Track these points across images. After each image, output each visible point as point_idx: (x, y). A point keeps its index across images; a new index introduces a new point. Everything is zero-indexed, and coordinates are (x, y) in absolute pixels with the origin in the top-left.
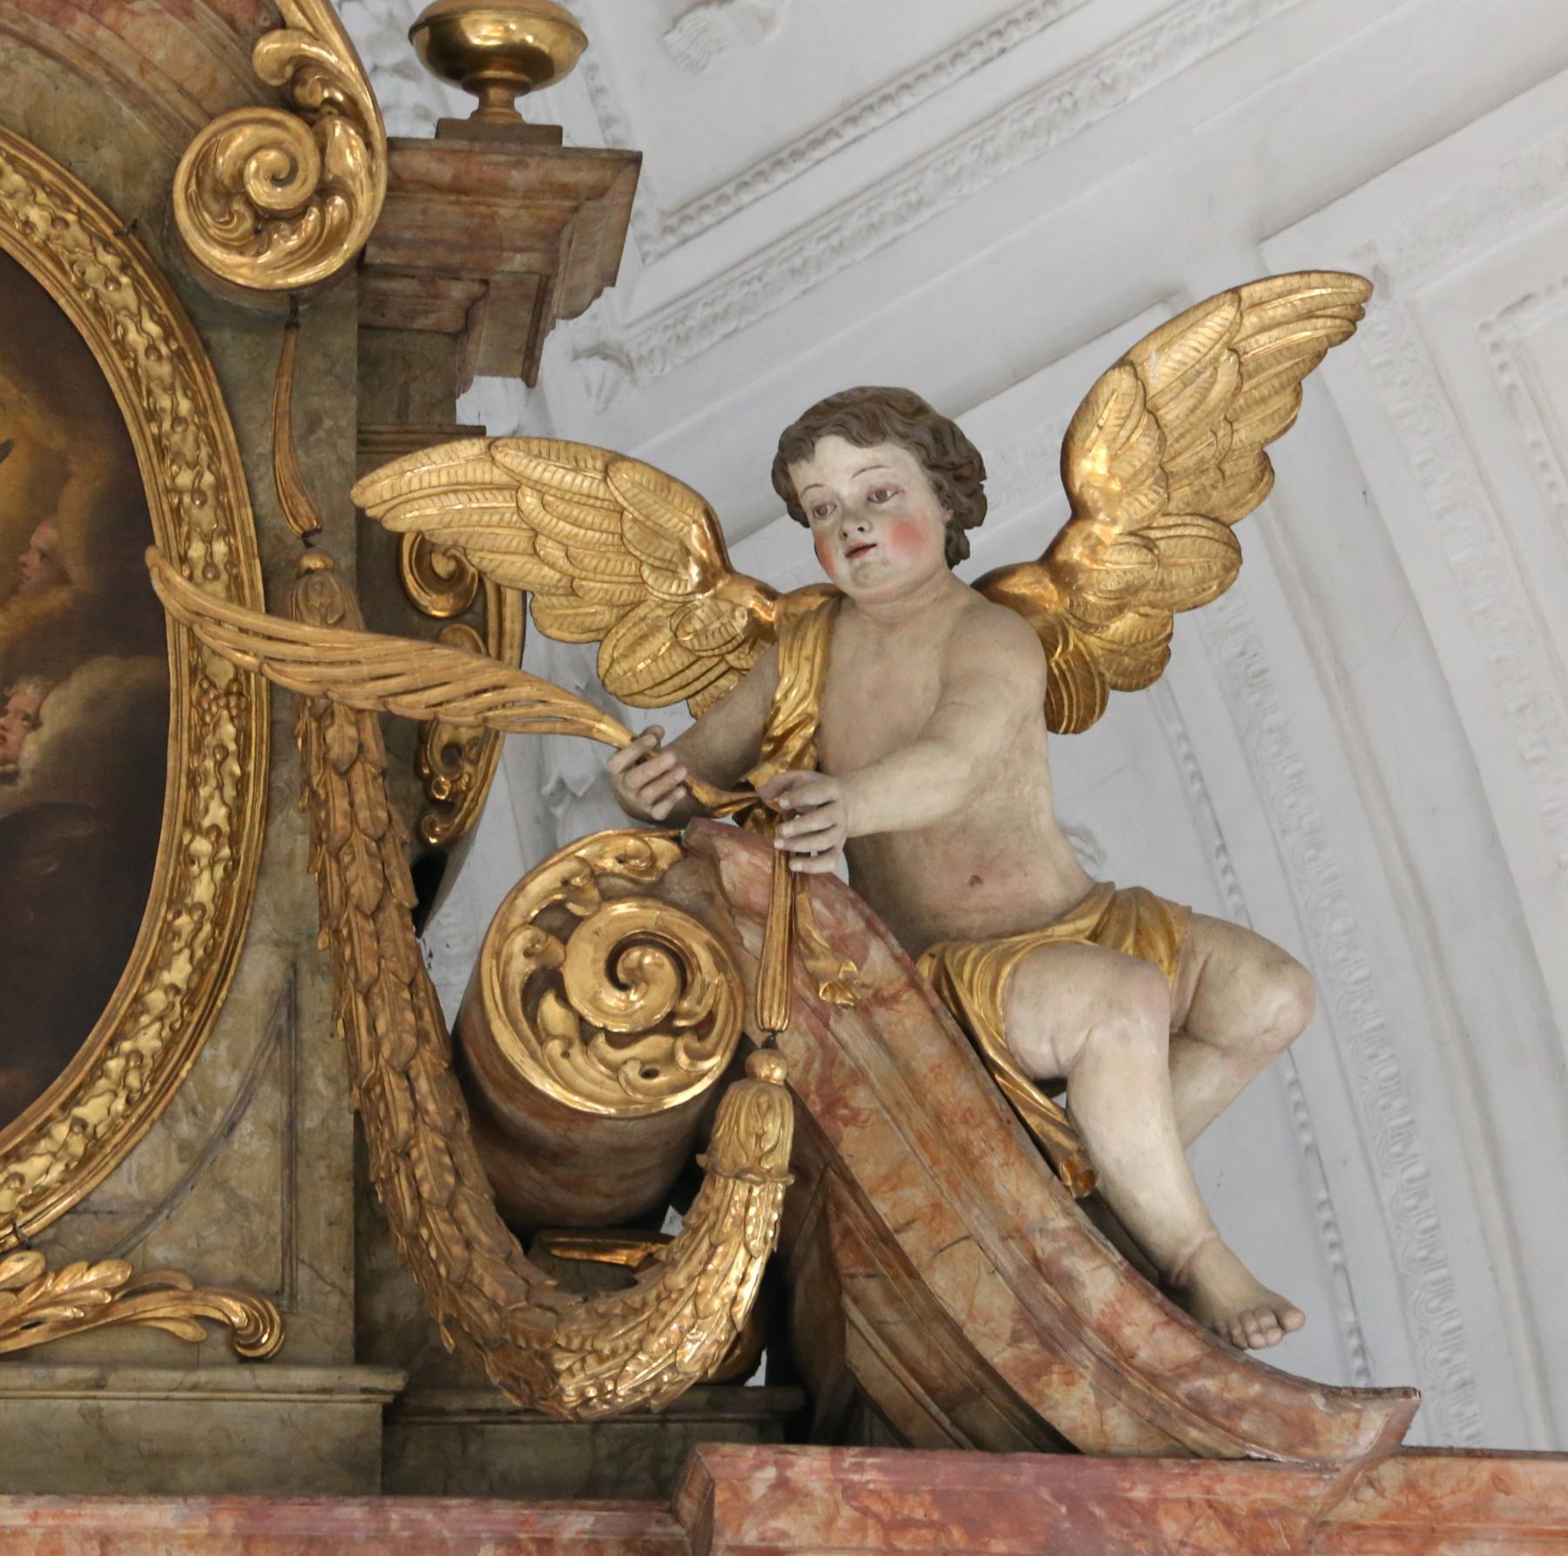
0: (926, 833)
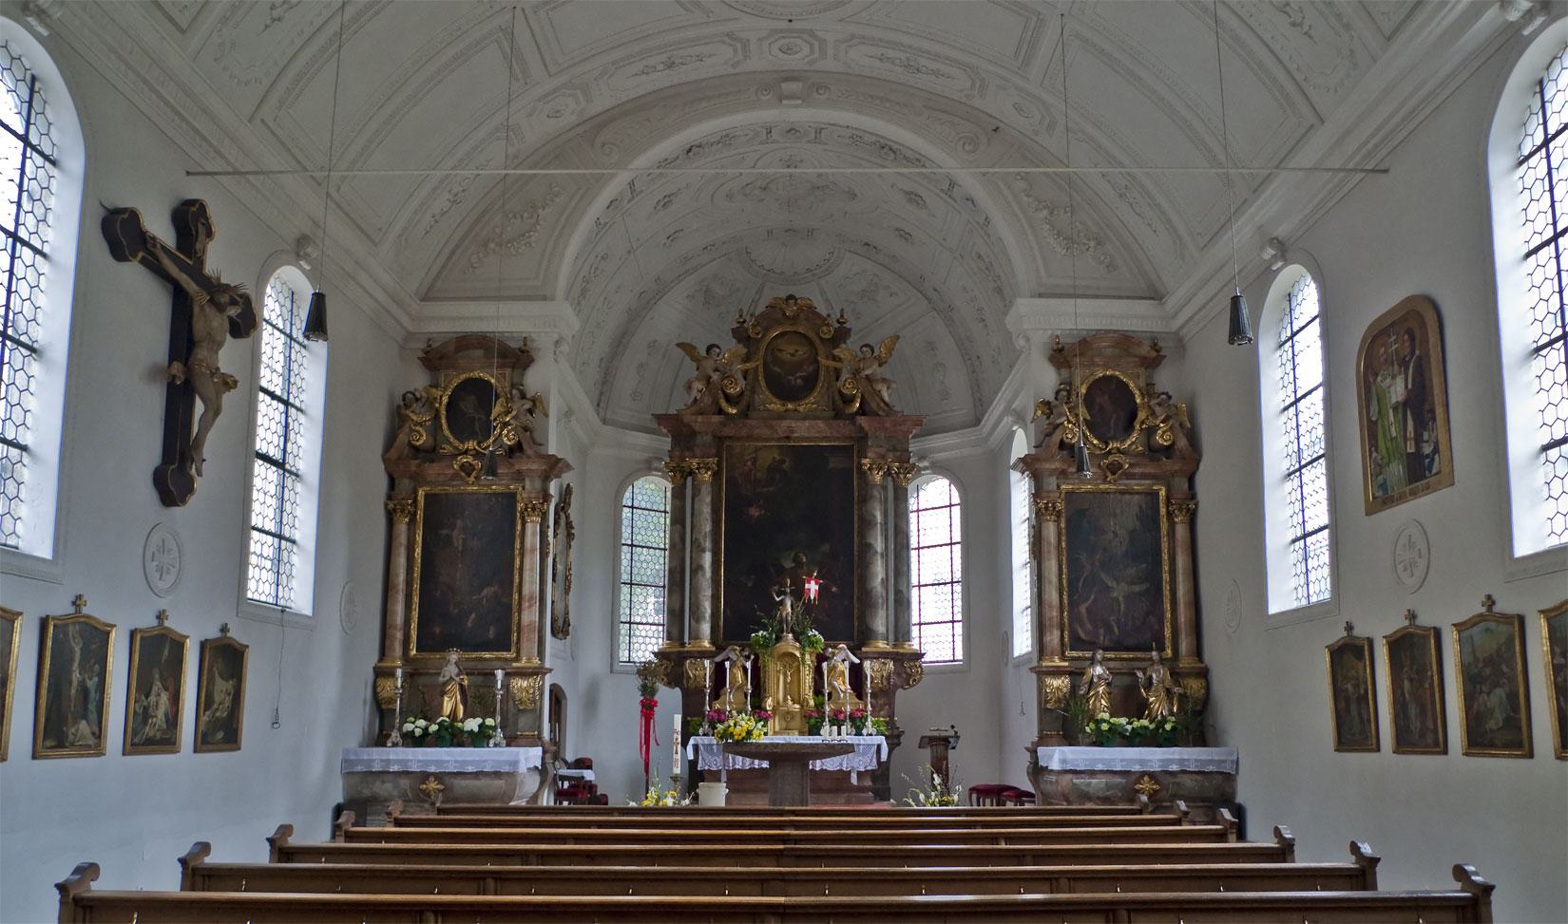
0: (872, 374)
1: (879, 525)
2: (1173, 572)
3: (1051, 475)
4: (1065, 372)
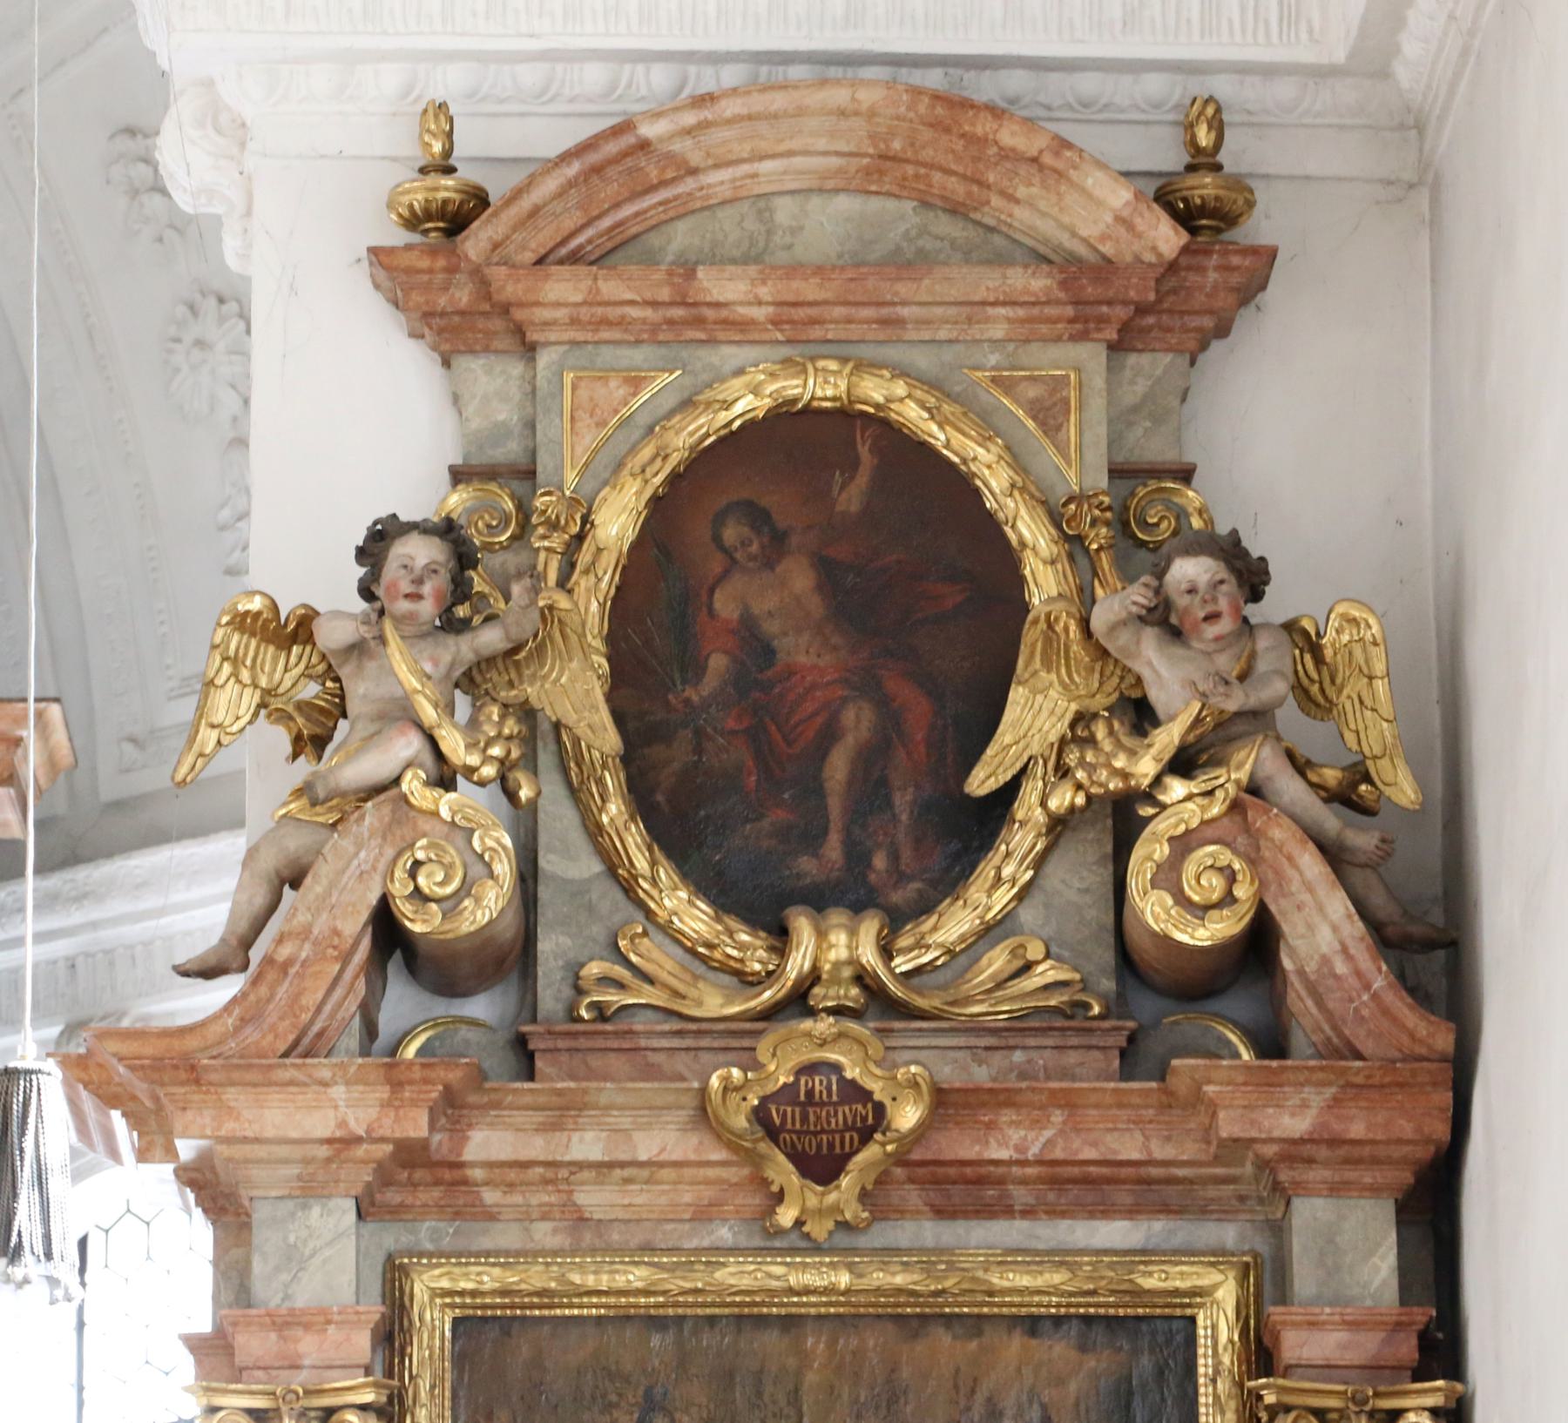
3: (309, 1190)
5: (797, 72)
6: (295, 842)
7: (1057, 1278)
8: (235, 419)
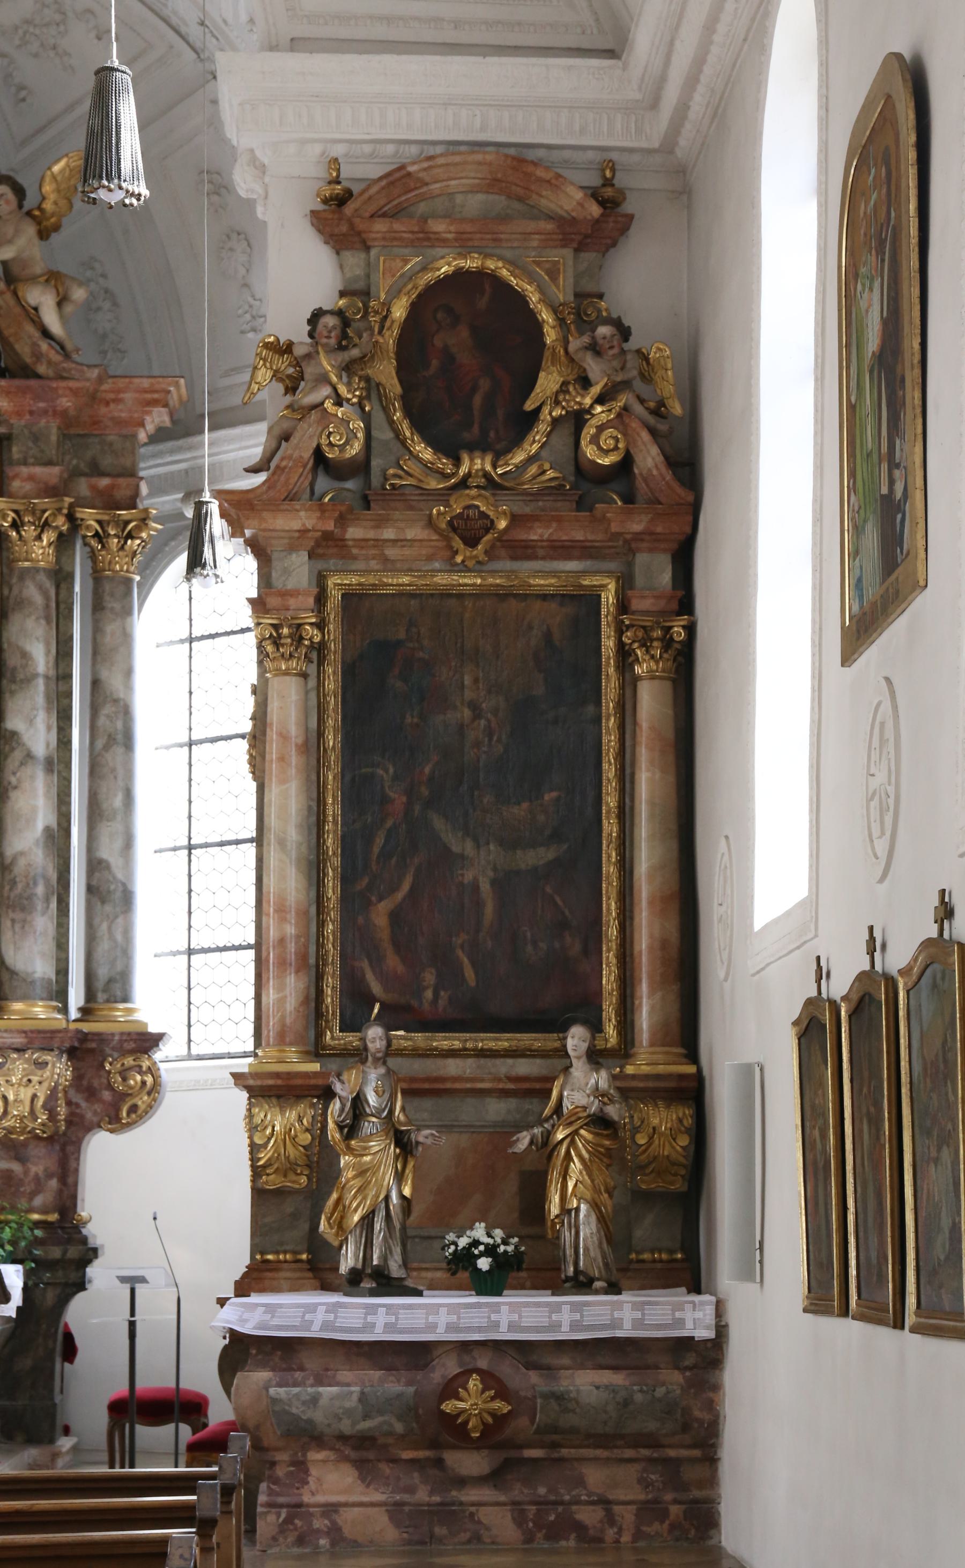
0: (14, 259)
1: (41, 682)
2: (625, 814)
3: (292, 548)
4: (354, 260)
5: (463, 148)
6: (286, 425)
7: (553, 581)
8: (244, 277)
